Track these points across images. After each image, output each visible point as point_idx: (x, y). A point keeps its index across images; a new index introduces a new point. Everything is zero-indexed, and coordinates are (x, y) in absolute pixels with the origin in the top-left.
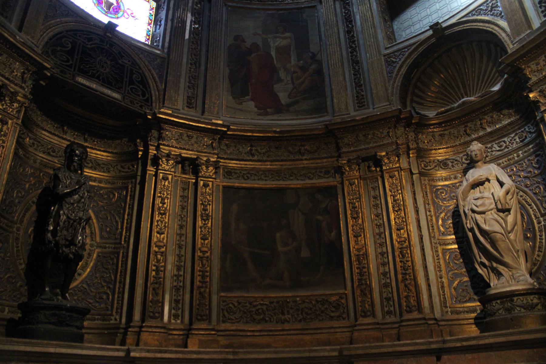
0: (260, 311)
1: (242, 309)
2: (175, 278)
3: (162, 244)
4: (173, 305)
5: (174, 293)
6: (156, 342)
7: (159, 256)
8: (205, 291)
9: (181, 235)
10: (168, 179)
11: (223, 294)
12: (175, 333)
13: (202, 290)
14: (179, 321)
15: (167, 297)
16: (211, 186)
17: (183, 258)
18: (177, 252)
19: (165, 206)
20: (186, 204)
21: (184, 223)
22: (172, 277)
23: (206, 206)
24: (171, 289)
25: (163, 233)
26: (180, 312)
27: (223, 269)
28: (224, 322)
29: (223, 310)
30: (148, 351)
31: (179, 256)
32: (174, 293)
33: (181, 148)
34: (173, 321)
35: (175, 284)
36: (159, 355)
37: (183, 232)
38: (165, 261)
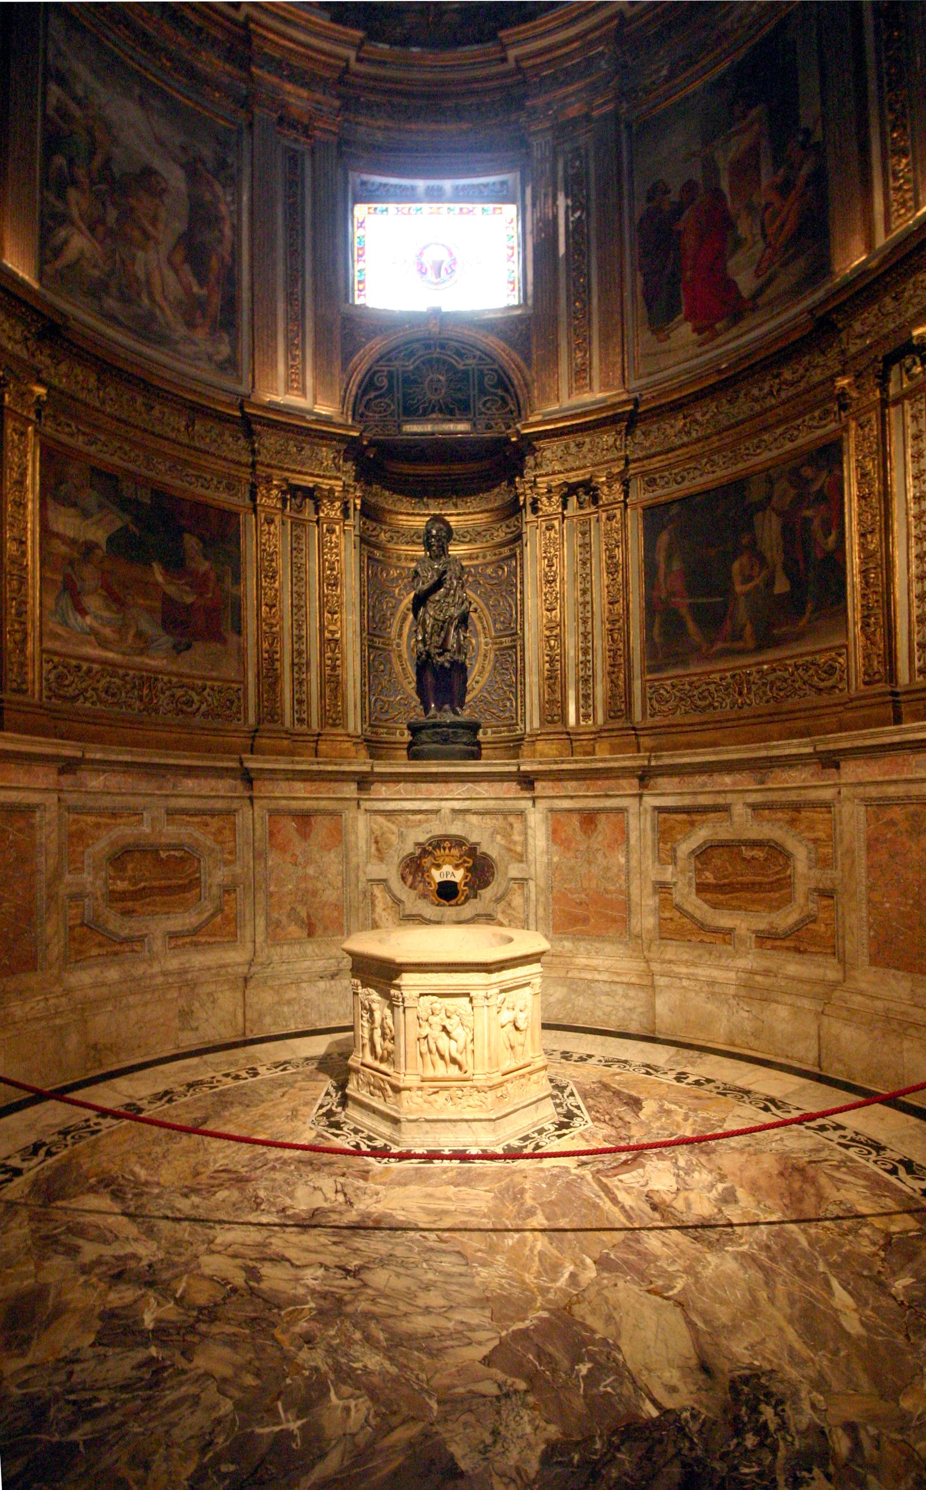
0: (706, 694)
1: (678, 694)
2: (581, 666)
3: (553, 625)
4: (581, 702)
5: (581, 686)
6: (555, 752)
7: (552, 642)
8: (618, 678)
9: (585, 604)
10: (553, 527)
11: (648, 677)
12: (582, 737)
13: (614, 676)
14: (590, 722)
15: (571, 694)
16: (619, 516)
17: (590, 637)
18: (581, 629)
19: (554, 568)
20: (588, 556)
21: (588, 586)
22: (577, 666)
23: (613, 550)
24: (577, 682)
25: (554, 609)
26: (591, 710)
27: (648, 641)
28: (652, 716)
29: (651, 699)
30: (541, 763)
31: (585, 635)
32: (581, 686)
33: (568, 471)
34: (582, 723)
35: (581, 674)
36: (555, 767)
37: (588, 598)
38: (562, 645)
